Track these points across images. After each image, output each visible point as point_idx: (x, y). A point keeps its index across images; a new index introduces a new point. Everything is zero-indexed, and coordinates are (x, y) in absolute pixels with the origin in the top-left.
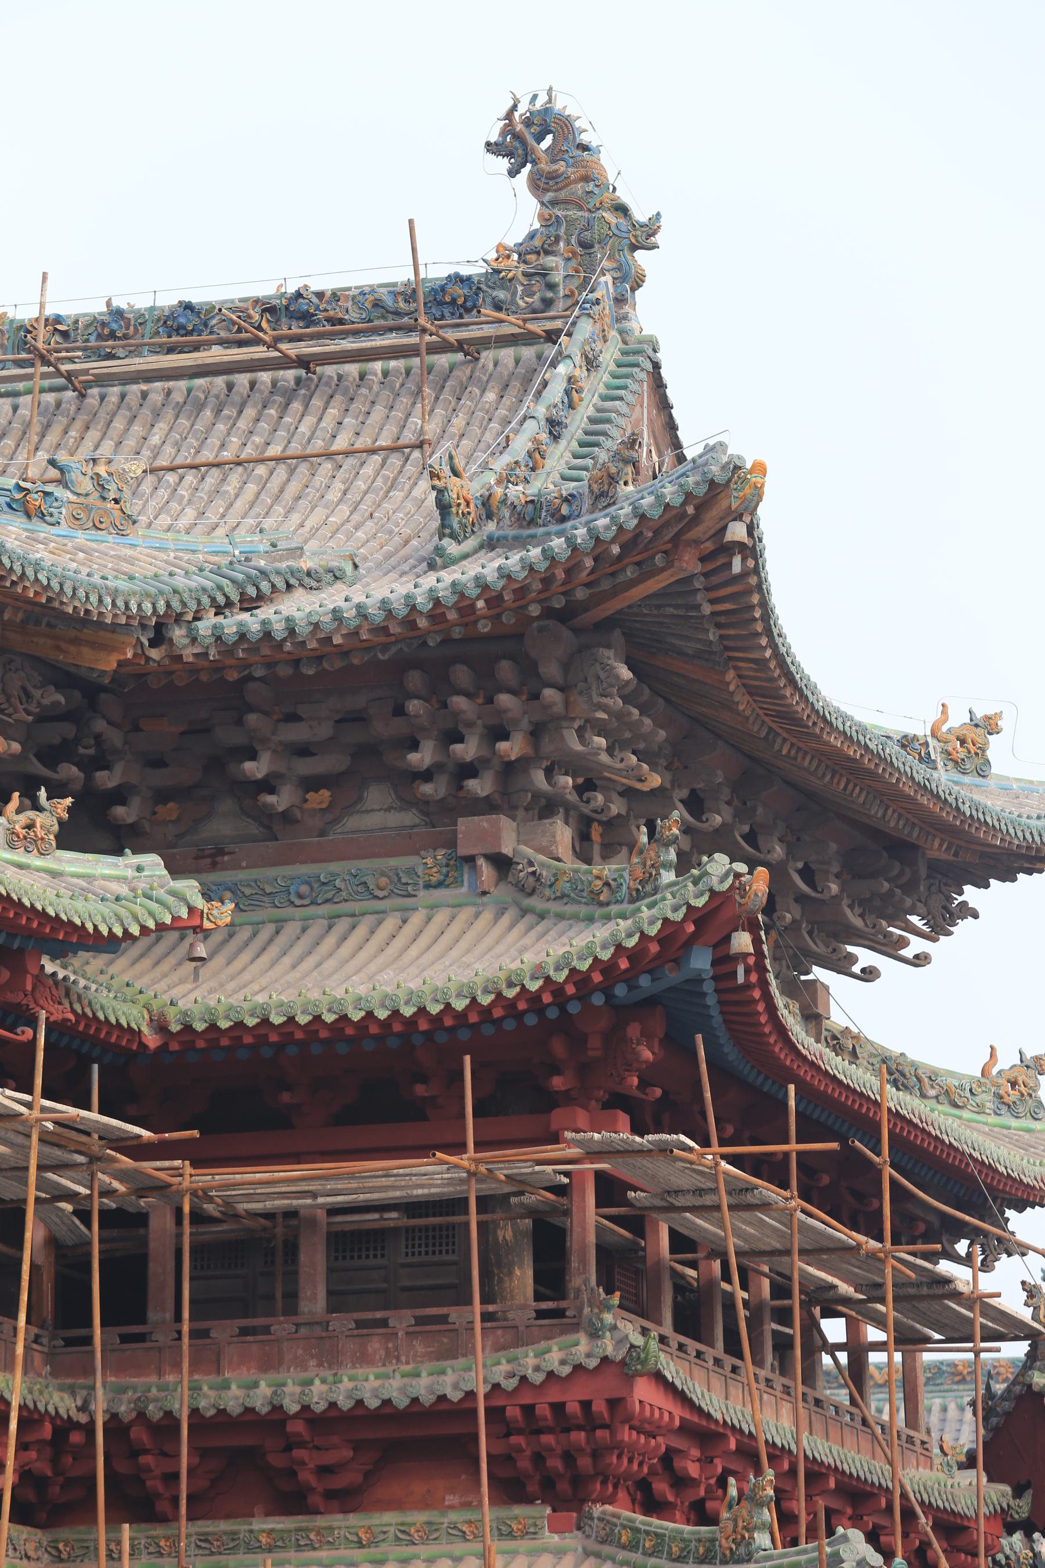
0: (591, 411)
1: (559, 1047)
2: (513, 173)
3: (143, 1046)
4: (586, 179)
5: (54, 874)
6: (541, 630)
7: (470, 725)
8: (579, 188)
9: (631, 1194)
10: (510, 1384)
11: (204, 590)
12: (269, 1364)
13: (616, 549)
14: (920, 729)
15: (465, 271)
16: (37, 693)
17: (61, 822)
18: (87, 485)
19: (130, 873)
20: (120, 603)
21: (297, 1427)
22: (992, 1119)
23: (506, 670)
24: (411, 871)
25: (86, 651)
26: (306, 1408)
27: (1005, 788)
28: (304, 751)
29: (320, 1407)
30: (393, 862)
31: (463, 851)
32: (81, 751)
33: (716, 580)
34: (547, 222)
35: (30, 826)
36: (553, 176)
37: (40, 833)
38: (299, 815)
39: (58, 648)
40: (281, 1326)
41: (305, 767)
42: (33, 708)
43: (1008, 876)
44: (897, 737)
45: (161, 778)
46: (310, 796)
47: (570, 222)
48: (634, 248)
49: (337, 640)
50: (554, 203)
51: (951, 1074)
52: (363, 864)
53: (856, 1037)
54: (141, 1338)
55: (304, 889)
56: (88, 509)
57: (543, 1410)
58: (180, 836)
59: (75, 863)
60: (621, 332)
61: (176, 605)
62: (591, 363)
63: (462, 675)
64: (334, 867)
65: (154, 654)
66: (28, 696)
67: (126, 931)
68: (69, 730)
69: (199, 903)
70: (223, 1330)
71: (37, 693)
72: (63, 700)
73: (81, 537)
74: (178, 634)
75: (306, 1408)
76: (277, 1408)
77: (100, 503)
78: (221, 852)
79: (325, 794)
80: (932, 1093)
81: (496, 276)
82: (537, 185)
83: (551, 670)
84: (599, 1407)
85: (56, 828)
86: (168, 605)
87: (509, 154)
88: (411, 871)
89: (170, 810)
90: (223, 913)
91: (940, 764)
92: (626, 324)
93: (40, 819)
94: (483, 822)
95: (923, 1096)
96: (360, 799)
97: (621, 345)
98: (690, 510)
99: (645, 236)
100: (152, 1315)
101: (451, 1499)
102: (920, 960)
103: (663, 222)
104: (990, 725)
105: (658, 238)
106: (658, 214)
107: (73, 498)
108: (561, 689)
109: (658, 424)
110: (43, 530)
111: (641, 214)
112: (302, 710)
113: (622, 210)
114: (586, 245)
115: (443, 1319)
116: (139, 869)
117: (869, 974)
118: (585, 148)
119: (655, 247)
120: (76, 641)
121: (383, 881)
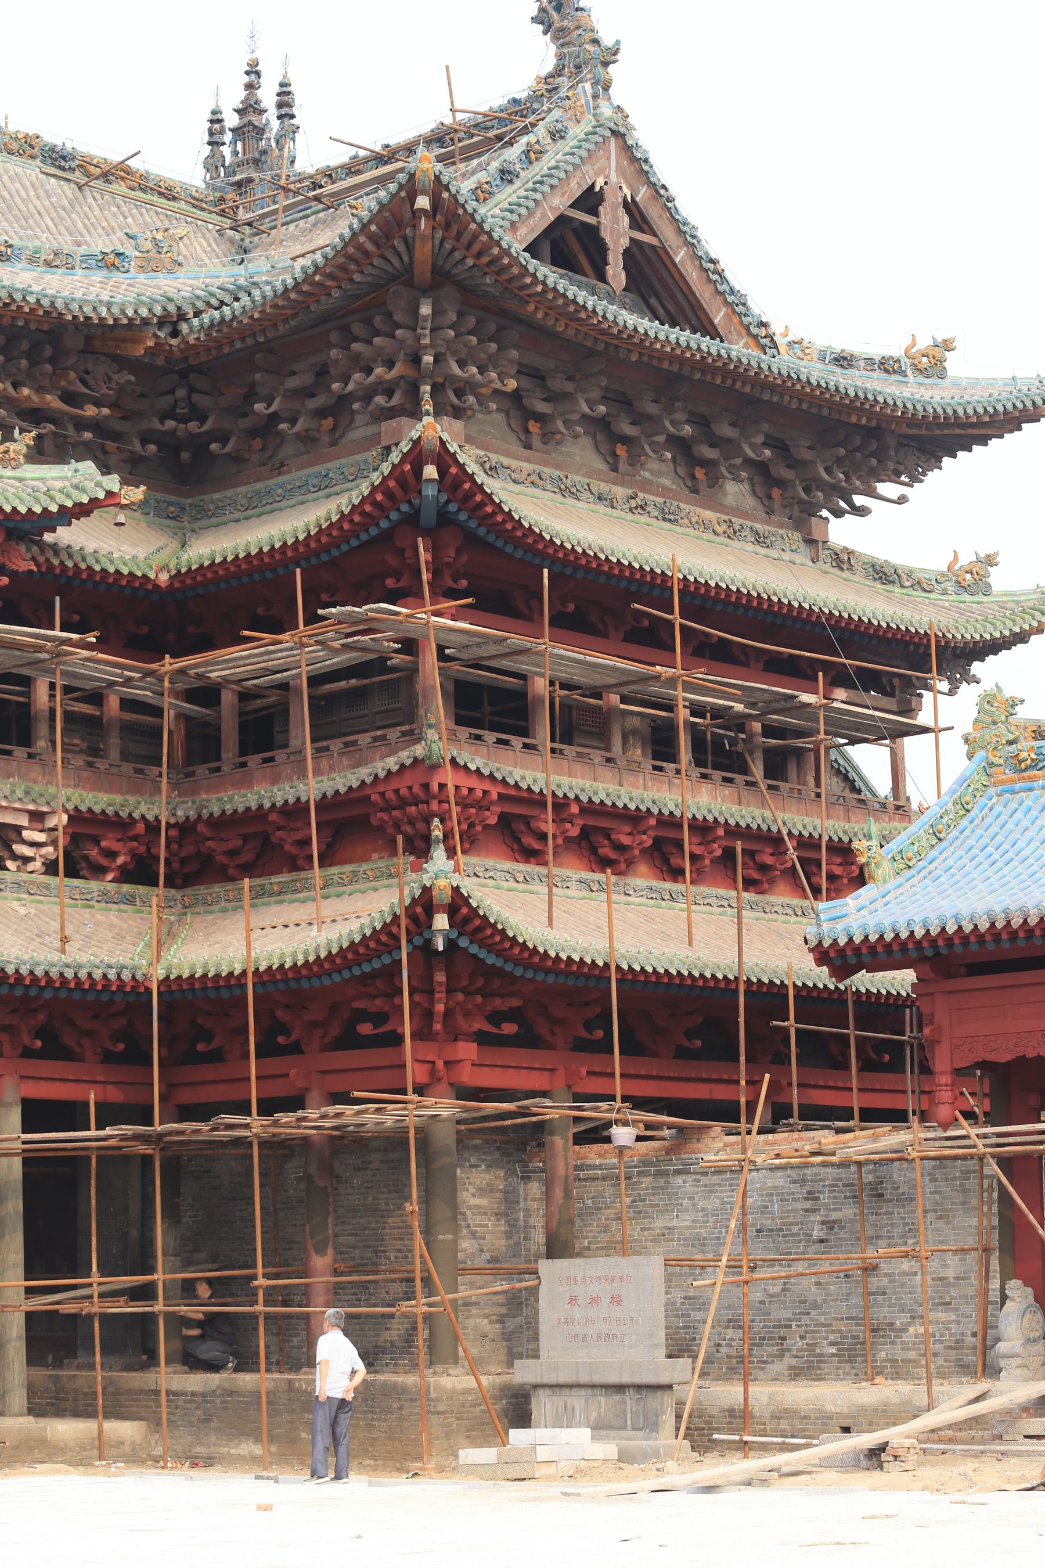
0: (553, 163)
1: (391, 560)
2: (545, 33)
3: (156, 586)
4: (578, 27)
5: (20, 480)
6: (395, 292)
7: (375, 361)
8: (575, 33)
9: (447, 651)
10: (369, 780)
11: (198, 297)
12: (274, 782)
13: (373, 228)
14: (897, 352)
15: (518, 97)
16: (115, 377)
17: (27, 446)
18: (148, 245)
19: (70, 474)
20: (115, 310)
21: (273, 817)
22: (954, 597)
23: (378, 320)
24: (365, 461)
25: (129, 345)
26: (273, 805)
27: (956, 384)
28: (308, 393)
29: (278, 804)
30: (358, 457)
31: (384, 443)
32: (178, 411)
33: (465, 240)
34: (560, 57)
35: (7, 452)
36: (561, 30)
37: (12, 455)
38: (316, 435)
39: (117, 347)
40: (280, 755)
41: (312, 404)
42: (113, 386)
43: (983, 441)
44: (877, 359)
45: (244, 423)
46: (323, 422)
47: (570, 54)
48: (606, 64)
49: (256, 316)
50: (562, 45)
51: (923, 570)
52: (343, 461)
53: (851, 553)
54: (218, 769)
55: (315, 481)
56: (149, 260)
57: (390, 795)
58: (270, 458)
59: (33, 472)
60: (594, 115)
61: (172, 308)
62: (557, 135)
63: (357, 329)
64: (329, 465)
65: (174, 342)
66: (110, 379)
67: (45, 510)
68: (169, 399)
69: (115, 487)
70: (254, 760)
71: (115, 377)
72: (132, 378)
73: (142, 278)
74: (184, 327)
75: (273, 805)
76: (261, 807)
77: (157, 256)
78: (282, 465)
79: (330, 419)
80: (908, 584)
81: (536, 97)
82: (555, 39)
83: (397, 317)
84: (416, 789)
85: (25, 450)
86: (165, 310)
87: (542, 23)
88: (365, 461)
89: (257, 443)
90: (137, 494)
91: (909, 373)
92: (599, 111)
93: (12, 446)
94: (393, 423)
95: (902, 586)
96: (352, 421)
97: (594, 123)
98: (403, 194)
99: (610, 56)
100: (224, 756)
101: (375, 856)
102: (902, 500)
103: (622, 47)
104: (947, 345)
105: (619, 57)
106: (618, 42)
107: (137, 254)
108: (408, 328)
109: (631, 170)
110: (118, 276)
111: (608, 41)
112: (296, 367)
113: (596, 42)
114: (578, 67)
115: (355, 743)
116: (76, 471)
117: (861, 512)
118: (582, 9)
119: (614, 62)
120: (125, 340)
121: (352, 470)
